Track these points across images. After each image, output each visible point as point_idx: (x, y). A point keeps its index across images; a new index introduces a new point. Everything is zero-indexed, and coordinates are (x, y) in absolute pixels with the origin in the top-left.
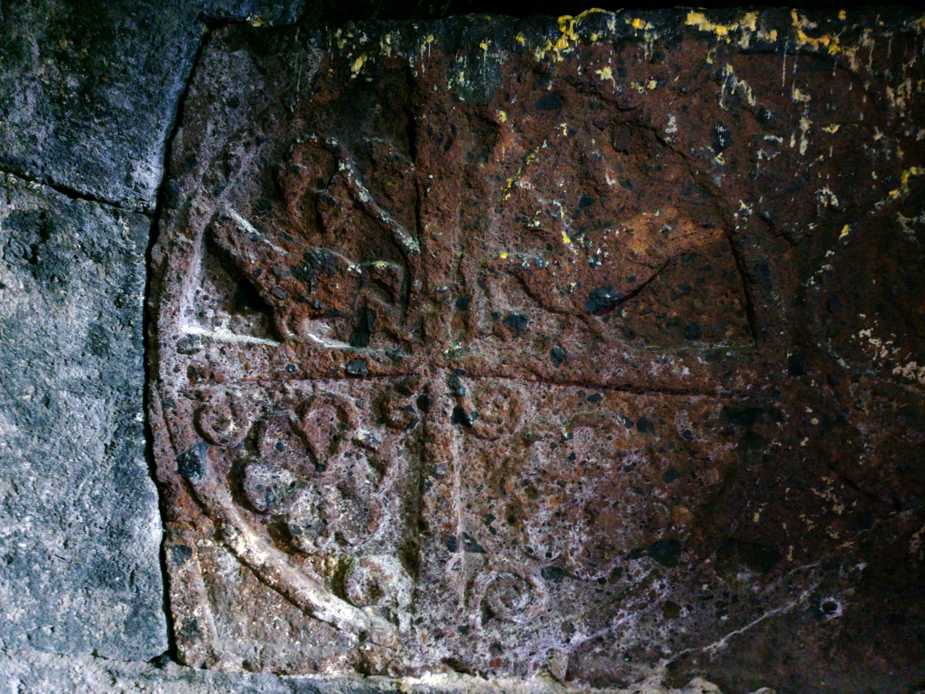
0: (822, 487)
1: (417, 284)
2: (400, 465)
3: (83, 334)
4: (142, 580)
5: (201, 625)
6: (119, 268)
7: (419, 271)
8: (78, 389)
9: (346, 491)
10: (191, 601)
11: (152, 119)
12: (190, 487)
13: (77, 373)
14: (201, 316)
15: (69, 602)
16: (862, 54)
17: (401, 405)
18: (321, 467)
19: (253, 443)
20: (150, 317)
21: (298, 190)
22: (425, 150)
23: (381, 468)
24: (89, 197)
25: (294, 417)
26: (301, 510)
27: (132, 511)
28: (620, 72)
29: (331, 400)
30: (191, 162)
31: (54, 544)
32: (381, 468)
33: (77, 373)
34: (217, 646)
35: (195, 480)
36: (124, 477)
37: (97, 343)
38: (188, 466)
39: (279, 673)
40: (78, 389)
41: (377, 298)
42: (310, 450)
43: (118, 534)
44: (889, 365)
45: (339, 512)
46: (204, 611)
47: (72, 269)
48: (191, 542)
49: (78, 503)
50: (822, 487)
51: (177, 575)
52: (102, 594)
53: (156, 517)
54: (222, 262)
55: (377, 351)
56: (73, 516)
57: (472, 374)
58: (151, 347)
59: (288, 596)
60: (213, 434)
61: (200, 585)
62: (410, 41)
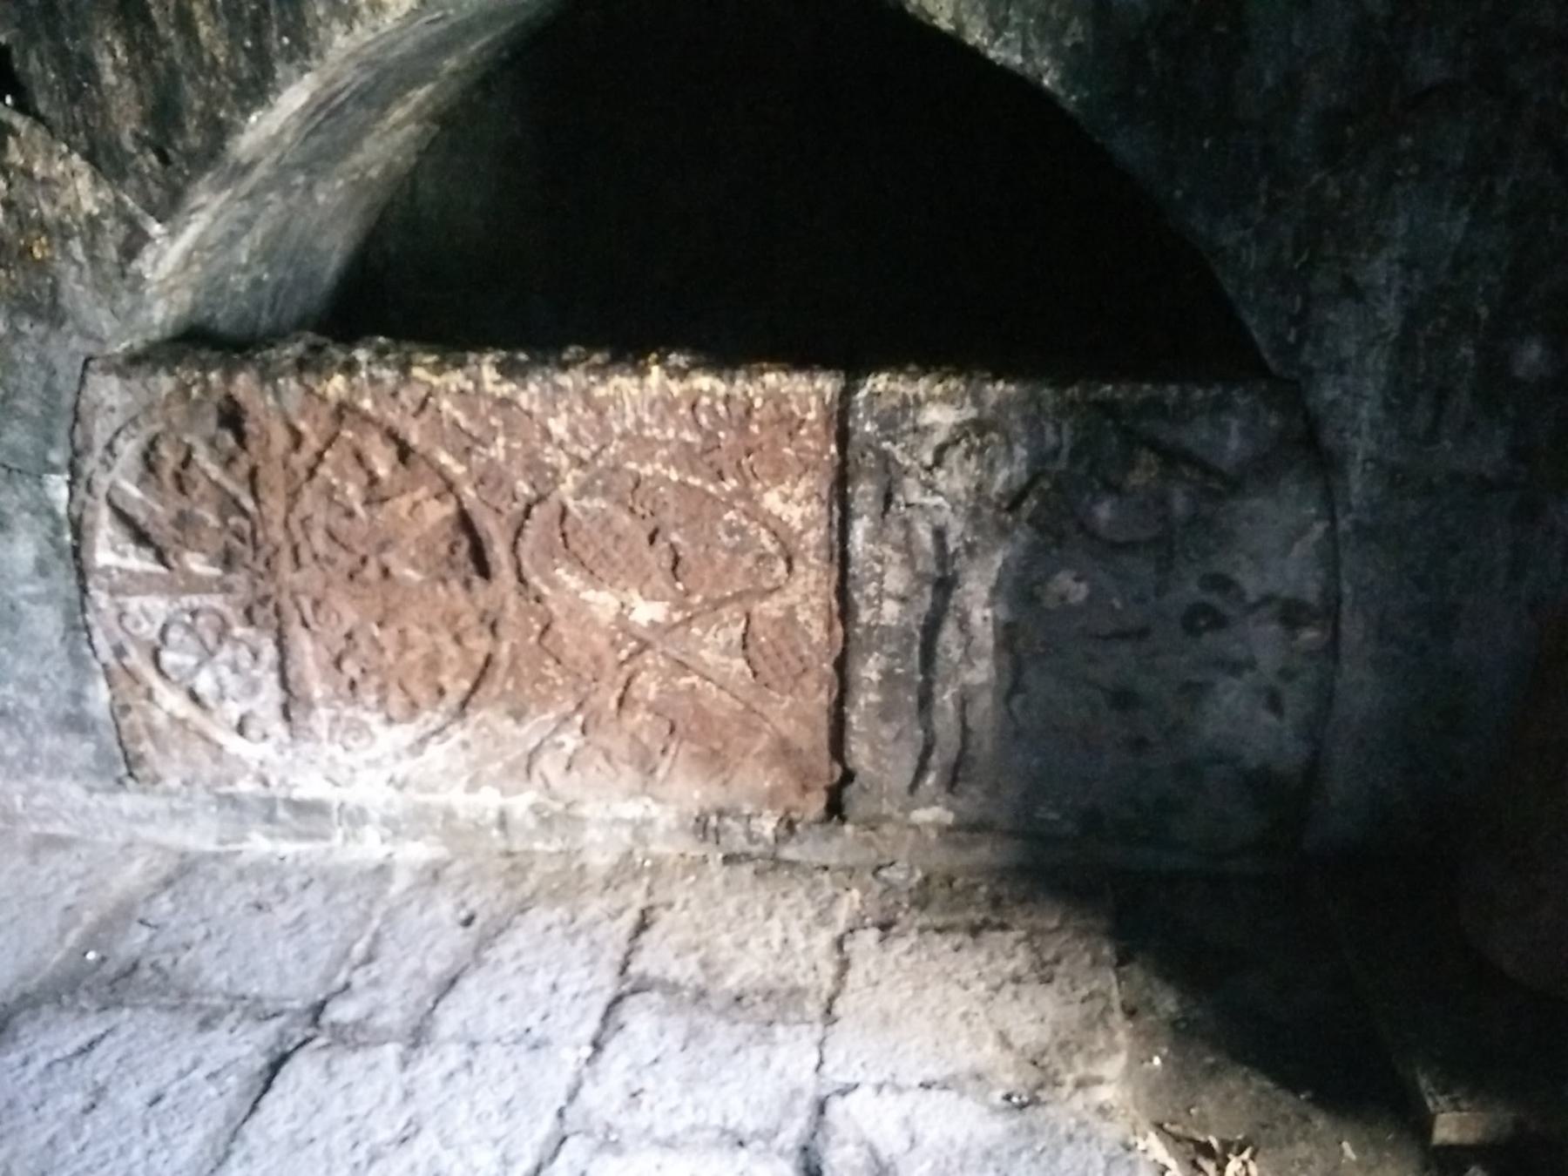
0: (547, 667)
1: (260, 535)
2: (269, 652)
3: (31, 564)
4: (101, 728)
5: (148, 757)
6: (49, 521)
7: (259, 524)
8: (34, 599)
9: (235, 668)
10: (137, 740)
11: (55, 421)
12: (123, 666)
13: (30, 589)
14: (114, 549)
15: (50, 742)
16: (531, 399)
17: (265, 611)
18: (212, 654)
19: (163, 634)
20: (76, 552)
21: (166, 473)
22: (253, 446)
23: (256, 655)
24: (19, 471)
25: (188, 619)
26: (204, 683)
27: (83, 683)
28: (376, 403)
29: (214, 611)
30: (89, 448)
31: (33, 702)
32: (256, 655)
33: (30, 589)
34: (160, 770)
35: (126, 661)
36: (77, 661)
37: (42, 568)
38: (120, 652)
39: (208, 788)
40: (34, 599)
41: (236, 543)
42: (202, 642)
43: (77, 697)
44: (577, 593)
45: (232, 683)
46: (146, 747)
47: (16, 520)
48: (130, 702)
49: (46, 676)
50: (547, 667)
51: (124, 723)
52: (73, 738)
53: (102, 684)
54: (123, 517)
55: (239, 579)
56: (44, 684)
57: (305, 592)
58: (82, 574)
59: (206, 738)
60: (134, 631)
61: (143, 731)
62: (228, 377)
